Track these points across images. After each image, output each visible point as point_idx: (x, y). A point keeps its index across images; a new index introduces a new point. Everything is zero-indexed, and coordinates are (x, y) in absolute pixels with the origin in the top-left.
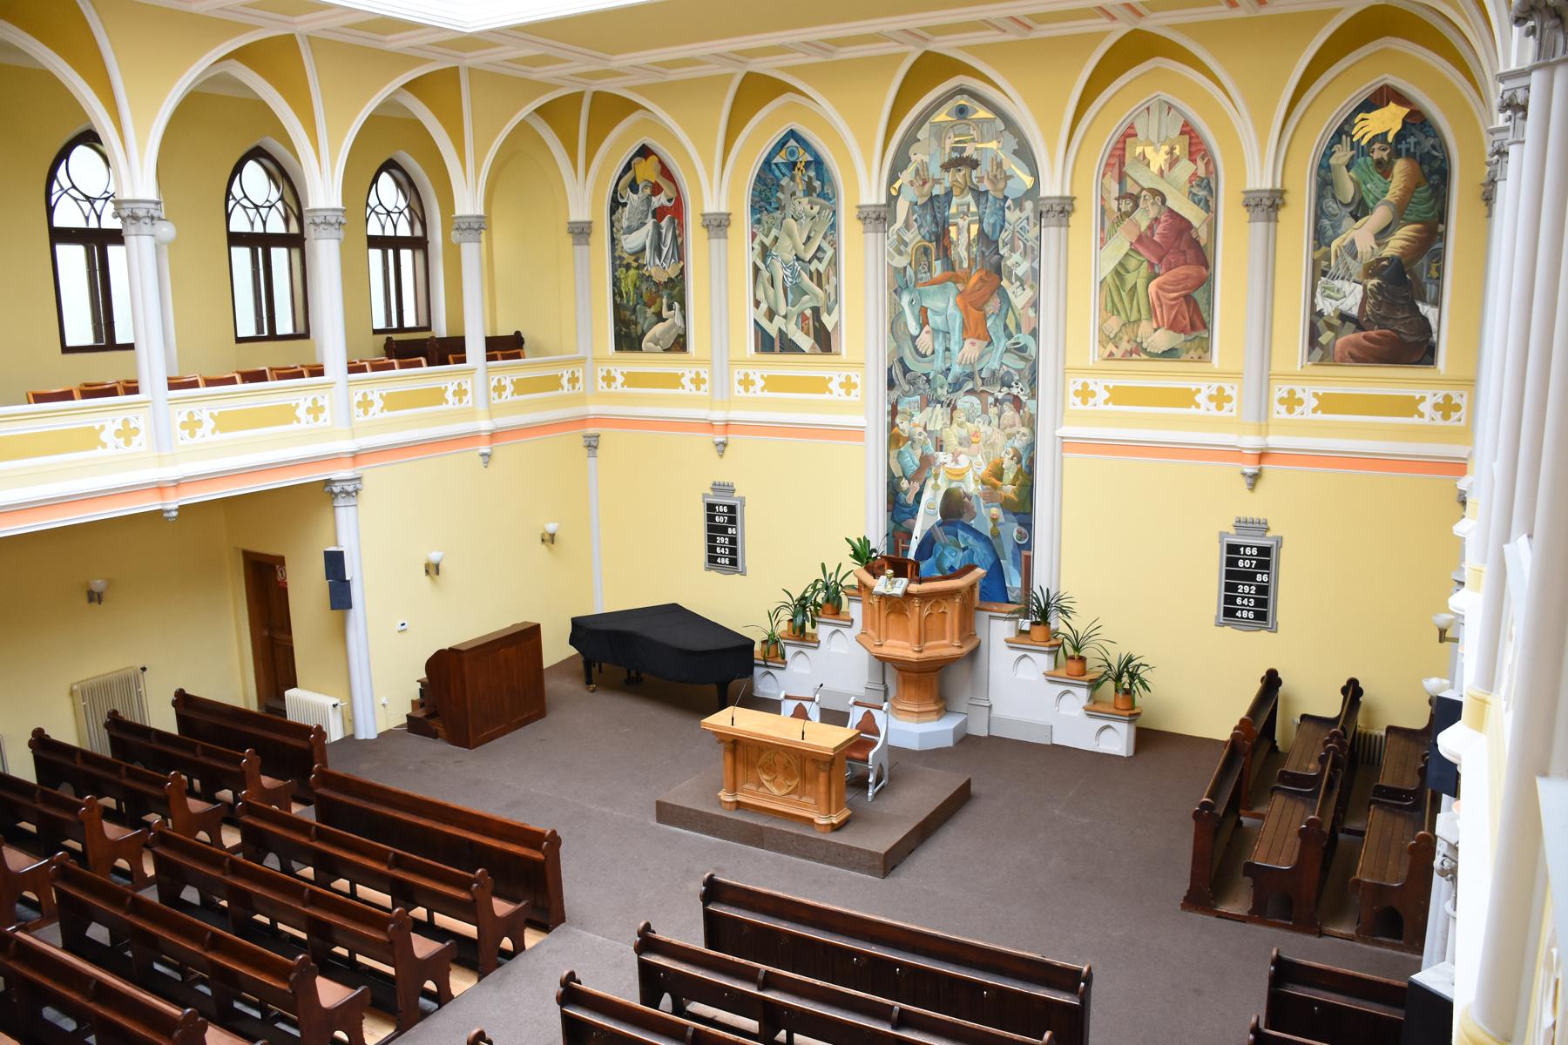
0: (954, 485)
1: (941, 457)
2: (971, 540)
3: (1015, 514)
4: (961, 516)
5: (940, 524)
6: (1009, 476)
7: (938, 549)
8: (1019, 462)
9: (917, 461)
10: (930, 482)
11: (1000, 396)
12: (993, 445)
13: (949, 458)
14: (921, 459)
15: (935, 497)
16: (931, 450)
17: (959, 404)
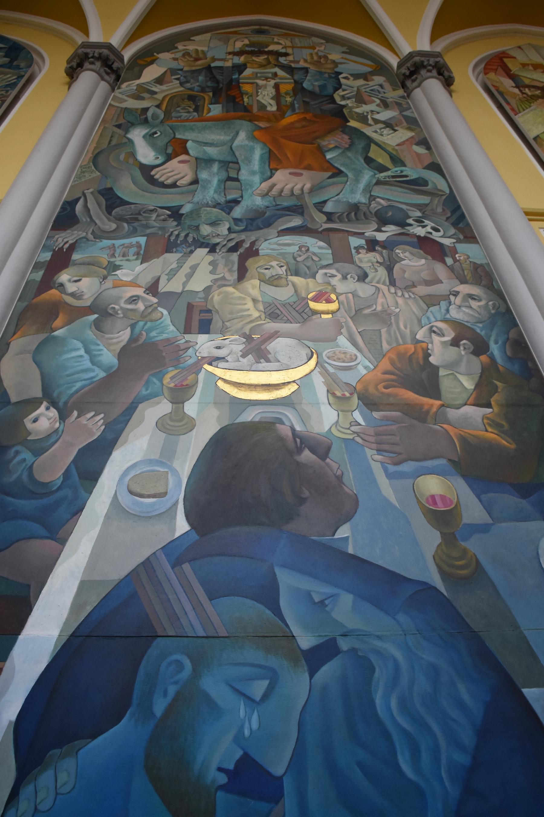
0: (249, 416)
1: (204, 344)
2: (346, 609)
3: (524, 490)
6: (461, 380)
8: (480, 348)
9: (109, 358)
11: (381, 237)
12: (385, 317)
13: (234, 345)
14: (124, 353)
16: (167, 326)
17: (264, 248)
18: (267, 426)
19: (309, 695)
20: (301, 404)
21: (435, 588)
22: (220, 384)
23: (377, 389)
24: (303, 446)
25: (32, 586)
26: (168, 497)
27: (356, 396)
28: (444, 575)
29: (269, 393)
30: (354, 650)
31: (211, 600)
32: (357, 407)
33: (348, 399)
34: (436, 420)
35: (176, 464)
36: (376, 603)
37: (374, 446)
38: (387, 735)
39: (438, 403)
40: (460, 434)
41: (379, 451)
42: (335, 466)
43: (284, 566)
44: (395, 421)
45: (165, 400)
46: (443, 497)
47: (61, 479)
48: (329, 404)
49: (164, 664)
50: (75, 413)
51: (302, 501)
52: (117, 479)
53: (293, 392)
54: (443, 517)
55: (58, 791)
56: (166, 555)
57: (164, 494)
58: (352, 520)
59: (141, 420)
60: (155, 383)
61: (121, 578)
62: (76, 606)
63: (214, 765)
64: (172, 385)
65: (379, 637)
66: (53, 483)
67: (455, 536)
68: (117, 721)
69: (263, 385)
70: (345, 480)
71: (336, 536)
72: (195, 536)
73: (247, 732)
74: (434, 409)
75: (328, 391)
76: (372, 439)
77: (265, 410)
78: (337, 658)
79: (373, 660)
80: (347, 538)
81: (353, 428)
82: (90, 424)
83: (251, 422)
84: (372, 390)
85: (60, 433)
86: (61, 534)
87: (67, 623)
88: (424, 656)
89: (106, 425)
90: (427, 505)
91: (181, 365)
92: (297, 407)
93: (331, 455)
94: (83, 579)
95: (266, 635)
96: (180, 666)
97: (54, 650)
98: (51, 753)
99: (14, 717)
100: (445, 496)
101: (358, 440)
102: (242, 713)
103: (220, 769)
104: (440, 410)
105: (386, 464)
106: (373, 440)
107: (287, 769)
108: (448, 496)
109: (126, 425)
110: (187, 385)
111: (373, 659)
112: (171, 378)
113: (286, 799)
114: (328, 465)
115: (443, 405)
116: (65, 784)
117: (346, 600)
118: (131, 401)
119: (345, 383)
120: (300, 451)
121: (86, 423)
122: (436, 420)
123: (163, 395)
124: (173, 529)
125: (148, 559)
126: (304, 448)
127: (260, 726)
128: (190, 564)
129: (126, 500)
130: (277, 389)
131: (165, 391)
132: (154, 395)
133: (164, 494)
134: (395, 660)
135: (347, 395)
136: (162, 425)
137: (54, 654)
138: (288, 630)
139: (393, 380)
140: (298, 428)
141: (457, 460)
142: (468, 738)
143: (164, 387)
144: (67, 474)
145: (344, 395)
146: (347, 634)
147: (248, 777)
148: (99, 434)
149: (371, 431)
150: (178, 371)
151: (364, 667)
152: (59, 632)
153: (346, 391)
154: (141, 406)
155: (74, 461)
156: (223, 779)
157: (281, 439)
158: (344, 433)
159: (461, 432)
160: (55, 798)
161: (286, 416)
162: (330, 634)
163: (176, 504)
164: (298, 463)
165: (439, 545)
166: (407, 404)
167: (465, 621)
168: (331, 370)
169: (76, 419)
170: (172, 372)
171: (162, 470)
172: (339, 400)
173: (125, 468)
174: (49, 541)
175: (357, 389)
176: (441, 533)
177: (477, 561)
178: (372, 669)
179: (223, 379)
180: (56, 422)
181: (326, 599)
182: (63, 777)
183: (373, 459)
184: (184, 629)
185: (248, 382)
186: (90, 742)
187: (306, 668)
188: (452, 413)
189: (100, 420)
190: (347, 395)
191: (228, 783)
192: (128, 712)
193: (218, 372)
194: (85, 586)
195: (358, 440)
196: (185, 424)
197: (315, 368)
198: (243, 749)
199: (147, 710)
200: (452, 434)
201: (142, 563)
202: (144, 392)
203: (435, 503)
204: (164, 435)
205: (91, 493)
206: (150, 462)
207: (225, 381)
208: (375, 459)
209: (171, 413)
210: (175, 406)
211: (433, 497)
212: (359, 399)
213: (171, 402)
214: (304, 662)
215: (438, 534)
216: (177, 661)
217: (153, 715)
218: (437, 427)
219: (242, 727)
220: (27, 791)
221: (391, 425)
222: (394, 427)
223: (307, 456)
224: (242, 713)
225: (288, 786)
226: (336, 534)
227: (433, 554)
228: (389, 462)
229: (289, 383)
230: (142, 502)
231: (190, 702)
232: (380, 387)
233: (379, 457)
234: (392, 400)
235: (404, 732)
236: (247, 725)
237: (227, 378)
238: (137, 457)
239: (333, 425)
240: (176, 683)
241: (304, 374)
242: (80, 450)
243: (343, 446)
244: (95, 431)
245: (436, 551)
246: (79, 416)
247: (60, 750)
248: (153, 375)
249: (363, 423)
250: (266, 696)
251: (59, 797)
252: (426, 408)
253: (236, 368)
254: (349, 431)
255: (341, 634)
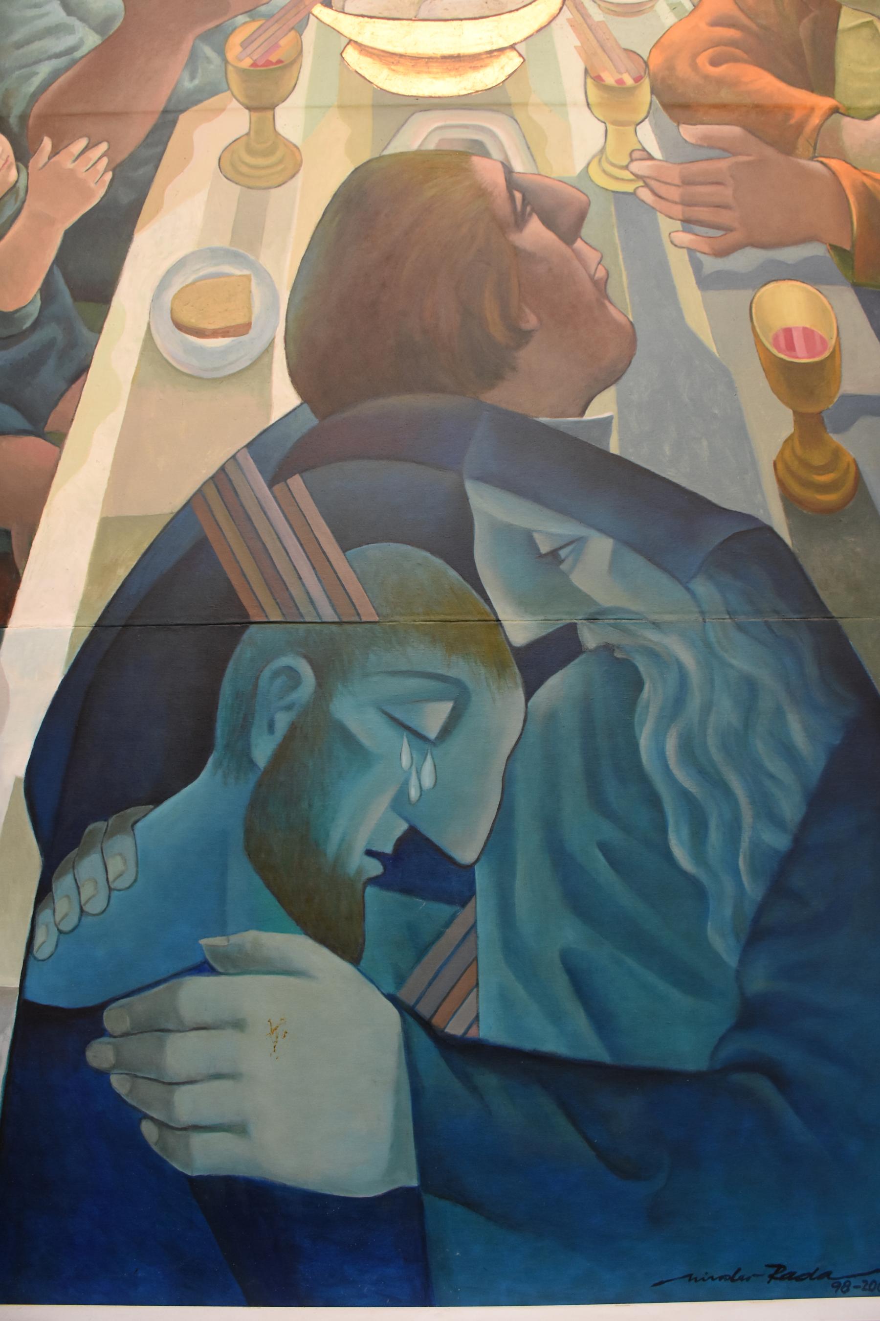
0: (416, 137)
2: (598, 567)
4: (493, 367)
5: (282, 456)
7: (270, 680)
10: (211, 132)
15: (245, 239)
18: (453, 161)
19: (523, 730)
20: (525, 105)
21: (770, 530)
22: (351, 56)
23: (694, 66)
24: (528, 209)
25: (13, 534)
26: (252, 333)
27: (646, 85)
28: (789, 501)
29: (458, 79)
30: (608, 648)
31: (344, 550)
32: (648, 113)
33: (630, 91)
34: (815, 149)
35: (266, 260)
36: (653, 555)
37: (678, 210)
38: (654, 801)
39: (826, 103)
40: (864, 185)
41: (688, 222)
42: (592, 257)
43: (483, 478)
44: (727, 149)
45: (235, 104)
46: (808, 333)
47: (38, 303)
48: (588, 104)
49: (266, 673)
50: (47, 144)
51: (522, 337)
52: (149, 295)
53: (510, 76)
54: (802, 379)
55: (112, 886)
56: (259, 461)
57: (243, 329)
58: (621, 381)
59: (186, 158)
60: (208, 60)
61: (176, 510)
62: (98, 569)
63: (360, 846)
64: (246, 63)
65: (656, 625)
66: (24, 311)
67: (822, 422)
68: (192, 775)
69: (444, 58)
70: (611, 291)
71: (589, 416)
72: (310, 420)
73: (414, 793)
74: (815, 120)
75: (586, 71)
76: (674, 193)
77: (449, 123)
78: (577, 661)
79: (641, 669)
80: (609, 420)
81: (636, 167)
82: (81, 168)
83: (418, 153)
84: (683, 69)
85: (22, 193)
86: (52, 424)
87: (85, 603)
88: (734, 662)
89: (114, 170)
90: (775, 351)
91: (263, 9)
92: (520, 115)
93: (585, 231)
94: (104, 515)
95: (448, 618)
96: (293, 678)
97: (69, 653)
98: (91, 827)
99: (22, 772)
100: (813, 332)
101: (645, 195)
102: (405, 761)
103: (370, 853)
104: (829, 122)
105: (698, 254)
106: (677, 198)
107: (481, 853)
108: (820, 331)
109: (157, 167)
110: (280, 61)
111: (642, 664)
112: (245, 45)
113: (478, 900)
114: (578, 254)
115: (835, 110)
116: (121, 875)
117: (601, 547)
118: (161, 109)
119: (625, 50)
120: (520, 221)
121: (70, 165)
122: (815, 149)
123: (229, 89)
124: (268, 406)
125: (222, 469)
126: (530, 215)
127: (436, 782)
128: (302, 477)
129: (171, 344)
130: (475, 68)
131: (233, 77)
132: (210, 91)
133: (243, 329)
134: (681, 667)
135: (629, 81)
136: (229, 165)
137: (72, 661)
138: (487, 607)
139: (733, 43)
140: (518, 166)
141: (848, 248)
142: (791, 807)
143: (230, 68)
144: (47, 291)
145: (620, 82)
146: (598, 617)
147: (417, 865)
148: (102, 192)
149: (674, 174)
150: (255, 25)
151: (624, 677)
152: (74, 620)
153: (627, 71)
154: (184, 120)
155: (58, 260)
156: (375, 868)
157: (482, 193)
158: (617, 179)
159: (868, 182)
160: (109, 897)
161: (493, 135)
162: (564, 617)
163: (269, 350)
164: (517, 251)
165: (790, 439)
166: (757, 106)
167: (817, 596)
168: (596, 14)
169: (50, 158)
170: (244, 29)
171: (238, 272)
172: (609, 97)
173: (161, 272)
174: (32, 439)
175: (651, 67)
176: (795, 412)
177: (859, 478)
178: (639, 685)
179: (356, 42)
180: (9, 168)
181: (561, 548)
182: (115, 865)
183: (672, 242)
184: (298, 609)
185: (411, 50)
186: (152, 810)
187: (519, 680)
188: (854, 132)
189: (100, 158)
190: (629, 81)
191: (383, 874)
192: (211, 761)
193: (347, 25)
194: (109, 528)
195: (645, 195)
196: (281, 161)
197: (561, 9)
198: (406, 819)
199: (242, 758)
200: (846, 183)
201: (212, 478)
202: (188, 85)
203: (790, 347)
204: (238, 188)
205: (100, 331)
206: (214, 254)
207: (364, 49)
208: (677, 243)
209: (248, 134)
210: (255, 115)
211: (788, 332)
212: (653, 92)
213: (247, 108)
214: (517, 670)
215: (788, 415)
216: (290, 669)
217: (252, 763)
218: (815, 165)
219: (406, 784)
220: (63, 885)
221: (719, 158)
222: (723, 164)
223: (535, 234)
224: (405, 761)
225: (482, 879)
226: (587, 412)
227: (774, 458)
228: (707, 250)
229: (502, 50)
230: (202, 349)
231: (314, 740)
232: (703, 60)
233: (685, 238)
234: (725, 96)
235: (685, 795)
236: (414, 781)
237: (365, 39)
238: (186, 246)
239: (594, 157)
240: (289, 708)
241: (536, 27)
242: (67, 233)
243: (613, 209)
244: (92, 185)
245: (782, 452)
246: (55, 152)
247: (106, 823)
248: (205, 37)
249: (657, 153)
250: (446, 731)
251: (115, 894)
252: (797, 116)
253: (386, 14)
254: (626, 175)
255: (587, 616)
